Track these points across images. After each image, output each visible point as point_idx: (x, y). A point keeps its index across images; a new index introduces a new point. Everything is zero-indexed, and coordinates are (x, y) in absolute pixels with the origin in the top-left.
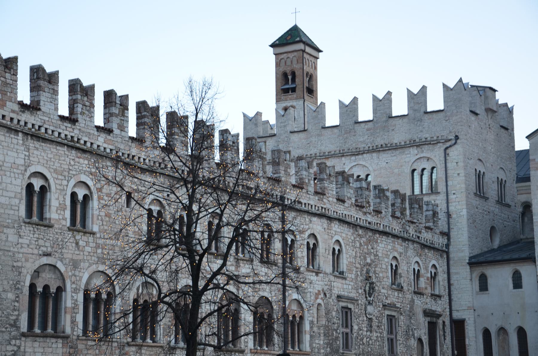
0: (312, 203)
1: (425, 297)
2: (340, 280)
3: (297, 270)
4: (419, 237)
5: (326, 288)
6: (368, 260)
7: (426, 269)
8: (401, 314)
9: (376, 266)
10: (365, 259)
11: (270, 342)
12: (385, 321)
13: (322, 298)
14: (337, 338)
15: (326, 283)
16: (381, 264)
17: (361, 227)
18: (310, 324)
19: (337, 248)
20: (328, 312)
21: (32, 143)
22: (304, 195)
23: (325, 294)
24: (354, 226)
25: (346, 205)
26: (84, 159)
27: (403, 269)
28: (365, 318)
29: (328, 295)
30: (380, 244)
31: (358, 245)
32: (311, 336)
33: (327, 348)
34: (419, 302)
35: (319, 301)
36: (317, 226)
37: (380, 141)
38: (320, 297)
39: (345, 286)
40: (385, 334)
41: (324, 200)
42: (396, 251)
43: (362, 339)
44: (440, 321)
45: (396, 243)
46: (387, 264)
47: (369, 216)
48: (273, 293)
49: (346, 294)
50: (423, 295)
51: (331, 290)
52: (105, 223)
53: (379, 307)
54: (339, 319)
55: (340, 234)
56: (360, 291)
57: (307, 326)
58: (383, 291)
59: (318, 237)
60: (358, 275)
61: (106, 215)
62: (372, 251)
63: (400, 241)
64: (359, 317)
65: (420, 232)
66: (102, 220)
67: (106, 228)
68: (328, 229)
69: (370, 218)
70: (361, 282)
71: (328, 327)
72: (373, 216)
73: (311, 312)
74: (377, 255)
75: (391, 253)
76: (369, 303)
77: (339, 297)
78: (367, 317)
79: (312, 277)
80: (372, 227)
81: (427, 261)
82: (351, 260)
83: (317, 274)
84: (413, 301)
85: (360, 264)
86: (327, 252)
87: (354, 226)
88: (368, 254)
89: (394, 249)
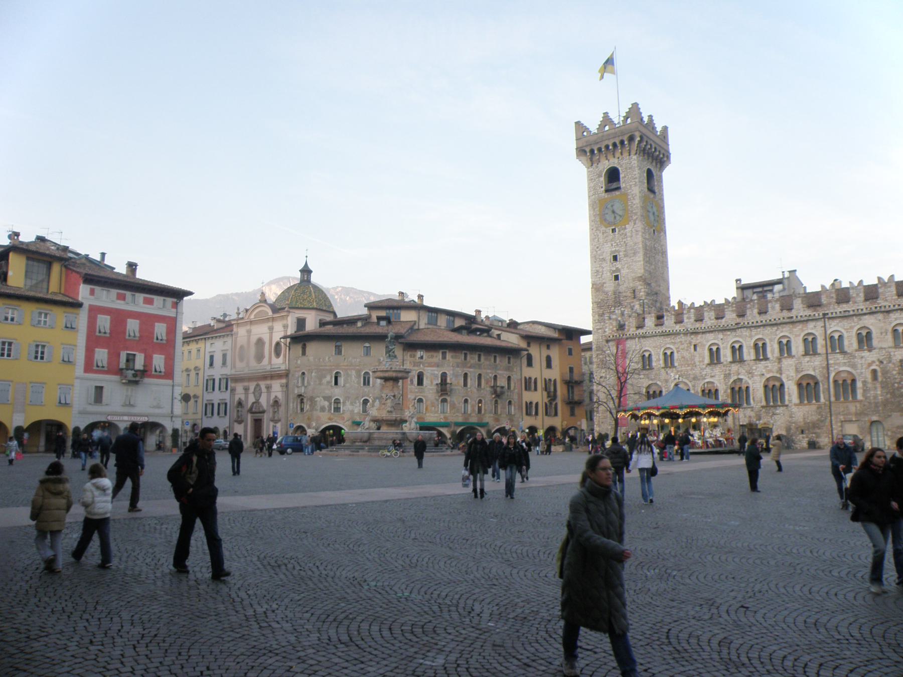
0: (861, 307)
5: (881, 358)
11: (817, 399)
21: (642, 340)
23: (881, 362)
32: (864, 391)
36: (869, 321)
51: (890, 357)
57: (859, 384)
59: (871, 327)
79: (866, 354)
83: (870, 351)
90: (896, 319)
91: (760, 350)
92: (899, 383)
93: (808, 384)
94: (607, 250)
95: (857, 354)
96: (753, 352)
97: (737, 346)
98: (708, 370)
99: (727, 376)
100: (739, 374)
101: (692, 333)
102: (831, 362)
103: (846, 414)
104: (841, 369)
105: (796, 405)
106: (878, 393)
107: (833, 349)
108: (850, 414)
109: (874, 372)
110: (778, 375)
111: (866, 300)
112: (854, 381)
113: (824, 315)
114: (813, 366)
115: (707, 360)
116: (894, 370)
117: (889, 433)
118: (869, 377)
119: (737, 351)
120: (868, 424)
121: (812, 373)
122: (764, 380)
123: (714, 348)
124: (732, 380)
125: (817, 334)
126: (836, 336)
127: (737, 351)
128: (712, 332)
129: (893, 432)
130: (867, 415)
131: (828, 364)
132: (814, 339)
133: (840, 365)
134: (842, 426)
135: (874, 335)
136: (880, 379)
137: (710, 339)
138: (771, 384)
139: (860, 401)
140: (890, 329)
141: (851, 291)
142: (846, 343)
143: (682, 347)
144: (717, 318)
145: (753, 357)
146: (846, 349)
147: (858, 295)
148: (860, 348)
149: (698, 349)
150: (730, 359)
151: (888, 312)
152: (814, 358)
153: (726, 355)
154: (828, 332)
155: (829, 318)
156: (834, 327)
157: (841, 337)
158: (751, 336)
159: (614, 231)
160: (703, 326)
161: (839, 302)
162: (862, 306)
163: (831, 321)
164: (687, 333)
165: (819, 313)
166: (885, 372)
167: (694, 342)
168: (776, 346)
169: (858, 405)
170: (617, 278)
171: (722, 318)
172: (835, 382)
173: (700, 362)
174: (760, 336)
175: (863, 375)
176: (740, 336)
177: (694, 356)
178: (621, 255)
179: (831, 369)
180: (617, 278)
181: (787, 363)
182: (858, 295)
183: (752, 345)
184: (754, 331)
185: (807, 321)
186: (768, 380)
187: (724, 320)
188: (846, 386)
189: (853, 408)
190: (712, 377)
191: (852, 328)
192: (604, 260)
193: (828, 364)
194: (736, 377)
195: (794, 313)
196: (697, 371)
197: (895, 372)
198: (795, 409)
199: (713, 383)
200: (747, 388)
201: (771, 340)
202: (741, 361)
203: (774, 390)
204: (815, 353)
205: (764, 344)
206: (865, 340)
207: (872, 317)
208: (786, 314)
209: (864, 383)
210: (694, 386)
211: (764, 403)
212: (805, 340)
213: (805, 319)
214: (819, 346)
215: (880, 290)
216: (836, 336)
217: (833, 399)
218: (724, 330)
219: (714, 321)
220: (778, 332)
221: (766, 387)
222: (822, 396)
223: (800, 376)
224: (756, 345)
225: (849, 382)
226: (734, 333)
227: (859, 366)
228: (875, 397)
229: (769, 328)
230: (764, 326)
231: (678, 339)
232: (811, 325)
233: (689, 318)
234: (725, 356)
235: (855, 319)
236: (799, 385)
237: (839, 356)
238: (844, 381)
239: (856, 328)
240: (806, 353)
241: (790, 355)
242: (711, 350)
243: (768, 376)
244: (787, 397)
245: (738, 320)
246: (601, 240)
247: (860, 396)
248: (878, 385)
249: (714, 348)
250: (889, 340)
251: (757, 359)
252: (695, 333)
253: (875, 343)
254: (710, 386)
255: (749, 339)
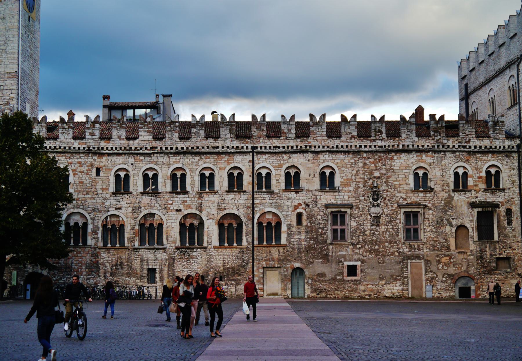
0: (292, 145)
1: (473, 192)
2: (332, 193)
3: (273, 193)
4: (464, 147)
5: (307, 201)
6: (377, 174)
7: (479, 170)
8: (430, 209)
9: (390, 177)
10: (371, 173)
11: (240, 241)
12: (401, 217)
13: (303, 208)
14: (322, 234)
15: (309, 197)
16: (398, 175)
17: (365, 152)
18: (287, 226)
19: (328, 172)
20: (310, 217)
22: (283, 141)
23: (308, 205)
24: (357, 152)
25: (343, 138)
26: (62, 156)
27: (435, 174)
28: (369, 217)
29: (311, 206)
30: (396, 161)
31: (361, 165)
32: (289, 235)
33: (310, 240)
34: (463, 197)
35: (299, 210)
36: (298, 160)
37: (497, 68)
38: (300, 207)
39: (337, 197)
40: (400, 226)
41: (308, 140)
42: (424, 162)
43: (365, 231)
44: (502, 210)
45: (424, 156)
46: (406, 174)
47: (380, 142)
48: (241, 210)
49: (339, 202)
50: (471, 191)
51: (316, 201)
52: (78, 187)
53: (392, 207)
54: (327, 221)
55: (333, 161)
56: (363, 198)
57: (284, 228)
58: (397, 195)
60: (359, 187)
61: (80, 183)
62: (384, 167)
63: (430, 154)
64: (358, 217)
65: (469, 142)
66: (76, 186)
67: (79, 189)
68: (313, 159)
69: (380, 143)
70: (364, 191)
71: (310, 227)
72: (387, 141)
73: (289, 218)
74: (393, 169)
75: (414, 165)
76: (373, 206)
77: (327, 206)
78: (371, 216)
79: (293, 195)
80: (381, 149)
81: (480, 164)
82: (350, 177)
83: (297, 192)
84: (451, 198)
85: (363, 179)
86: (312, 176)
87: (357, 152)
88: (376, 170)
89: (419, 161)
90: (324, 161)
91: (178, 183)
92: (323, 229)
93: (230, 225)
95: (285, 194)
96: (169, 183)
97: (151, 174)
98: (113, 201)
99: (136, 209)
100: (152, 207)
101: (95, 154)
102: (256, 201)
103: (269, 260)
104: (267, 210)
105: (215, 247)
106: (301, 238)
107: (260, 188)
108: (273, 260)
109: (299, 216)
110: (198, 212)
111: (297, 137)
112: (279, 224)
113: (254, 148)
114: (238, 204)
115: (112, 188)
116: (319, 214)
117: (310, 281)
118: (294, 219)
119: (150, 181)
120: (290, 271)
121: (236, 212)
122: (180, 217)
123: (122, 174)
124: (141, 215)
125: (243, 168)
126: (264, 172)
127: (150, 181)
128: (121, 154)
129: (313, 280)
130: (289, 261)
131: (253, 203)
132: (240, 175)
133: (265, 204)
134: (263, 273)
135: (302, 176)
136: (304, 224)
137: (118, 162)
138: (189, 221)
139: (285, 246)
140: (318, 171)
141: (283, 126)
142: (273, 181)
143: (80, 169)
144: (128, 139)
145: (169, 189)
146: (273, 188)
147: (289, 130)
148: (287, 189)
149: (102, 173)
150: (141, 189)
151: (318, 153)
152: (238, 196)
153: (137, 184)
154: (256, 168)
155: (258, 153)
156: (262, 161)
157: (269, 175)
158: (169, 165)
160: (110, 145)
161: (269, 137)
162: (294, 143)
163: (259, 156)
164: (88, 152)
165: (247, 145)
166: (310, 217)
167: (97, 164)
168: (197, 179)
169: (281, 250)
171: (135, 139)
172: (260, 224)
173: (103, 189)
174: (180, 165)
175: (288, 219)
176: (156, 163)
177: (96, 182)
179: (256, 209)
181: (207, 198)
182: (289, 130)
183: (169, 174)
184: (173, 159)
185: (234, 153)
186: (185, 217)
187: (137, 141)
188: (270, 230)
189: (275, 253)
190: (117, 209)
191: (281, 165)
193: (253, 203)
194: (146, 212)
195: (219, 143)
196: (98, 201)
197: (319, 217)
198: (214, 252)
199: (118, 216)
200: (161, 225)
201: (191, 171)
202: (155, 193)
203: (191, 231)
204: (240, 190)
205: (184, 176)
206: (293, 181)
207: (301, 155)
208: (212, 142)
209: (289, 226)
210: (93, 219)
211: (178, 244)
212: (230, 175)
213: (233, 150)
214: (245, 183)
215: (312, 129)
216: (264, 172)
217: (256, 242)
218: (136, 153)
219: (125, 143)
220: (200, 163)
221: (182, 225)
222: (244, 238)
223: (222, 215)
224: (173, 176)
225: (273, 224)
226: (148, 159)
227: (285, 208)
228: (299, 243)
229: (190, 157)
230: (185, 153)
231: (75, 159)
232: (238, 158)
233: (92, 134)
234: (135, 185)
235: (285, 157)
236: (220, 225)
237: (265, 195)
238: (269, 223)
239: (285, 167)
240: (231, 190)
241: (213, 191)
242: (117, 177)
243: (186, 212)
244: (206, 238)
245: (155, 143)
247: (283, 241)
248: (303, 230)
249: (122, 174)
250: (317, 183)
251: (174, 191)
252: (100, 153)
253: (302, 184)
254: (113, 219)
255: (165, 167)
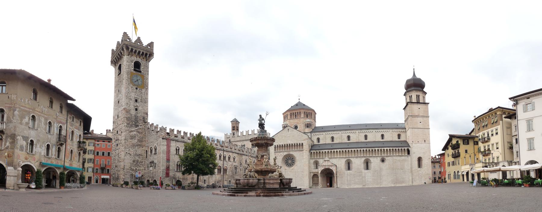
94: (133, 96)
159: (137, 89)
170: (136, 110)
178: (139, 100)
180: (136, 110)
192: (131, 99)
246: (130, 90)
